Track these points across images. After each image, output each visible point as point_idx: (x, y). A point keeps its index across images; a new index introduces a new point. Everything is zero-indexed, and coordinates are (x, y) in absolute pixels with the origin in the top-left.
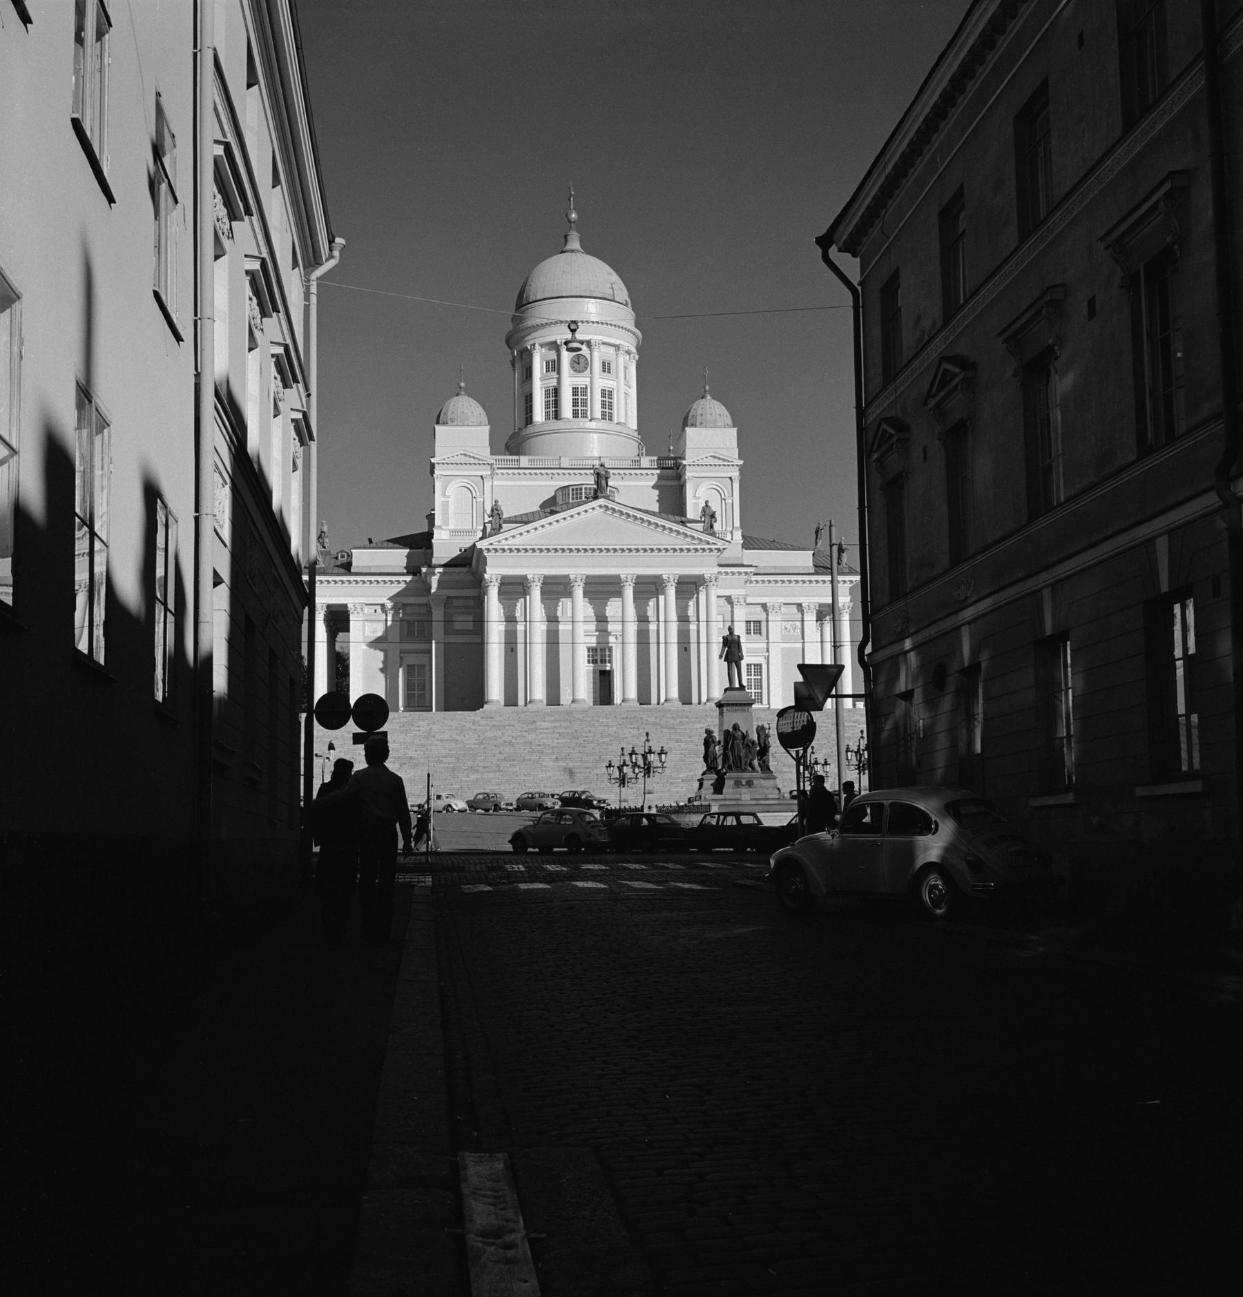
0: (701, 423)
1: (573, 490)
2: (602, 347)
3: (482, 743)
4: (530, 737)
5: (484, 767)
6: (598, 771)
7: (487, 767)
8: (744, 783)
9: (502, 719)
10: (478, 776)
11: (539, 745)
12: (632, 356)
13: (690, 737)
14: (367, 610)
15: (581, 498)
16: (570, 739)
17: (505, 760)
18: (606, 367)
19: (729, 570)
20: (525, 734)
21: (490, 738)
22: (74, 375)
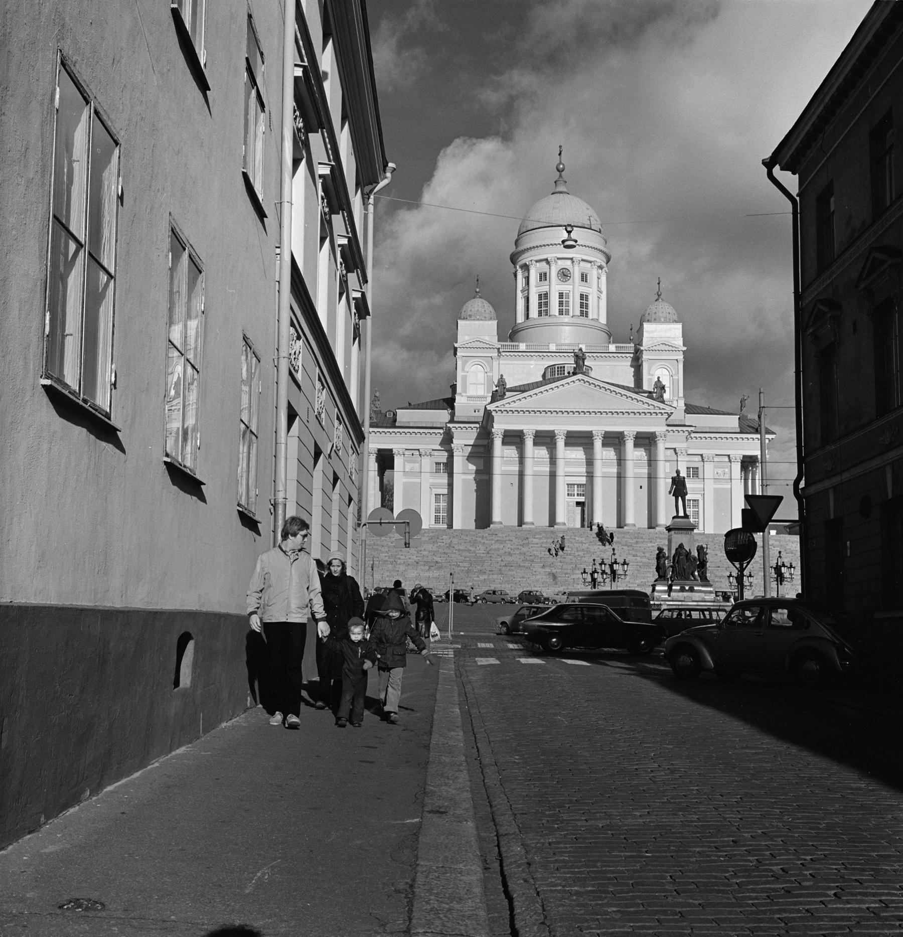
0: (655, 319)
1: (558, 368)
2: (582, 264)
3: (488, 553)
4: (524, 550)
5: (490, 571)
6: (574, 576)
7: (492, 571)
8: (687, 588)
12: (603, 270)
13: (644, 553)
15: (564, 374)
17: (505, 566)
18: (584, 278)
19: (675, 428)
20: (520, 547)
21: (495, 550)
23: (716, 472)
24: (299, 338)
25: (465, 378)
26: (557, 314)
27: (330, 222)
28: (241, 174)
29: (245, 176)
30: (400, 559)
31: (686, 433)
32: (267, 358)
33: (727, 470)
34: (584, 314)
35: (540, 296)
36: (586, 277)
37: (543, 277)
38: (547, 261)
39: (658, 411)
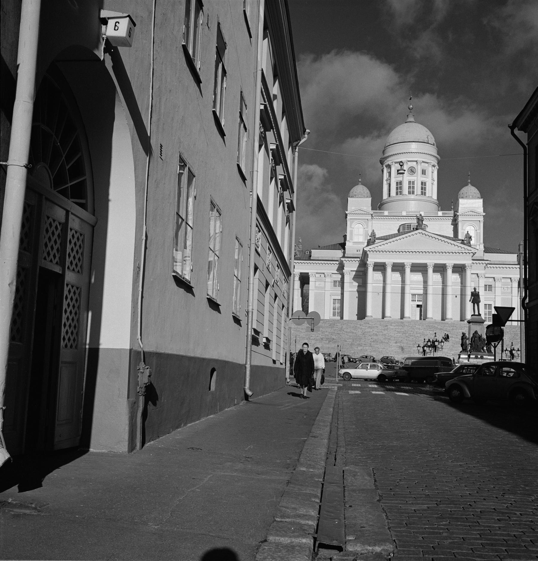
0: (466, 197)
1: (407, 225)
2: (423, 164)
3: (364, 334)
4: (385, 332)
5: (364, 344)
7: (365, 344)
8: (479, 357)
9: (373, 324)
10: (361, 348)
11: (389, 336)
12: (435, 167)
13: (457, 336)
14: (318, 275)
15: (411, 229)
16: (403, 334)
17: (374, 341)
18: (424, 172)
19: (477, 262)
20: (382, 331)
21: (368, 332)
22: (210, 199)
24: (259, 231)
25: (351, 232)
27: (275, 170)
29: (238, 165)
30: (312, 336)
31: (485, 265)
32: (245, 245)
34: (423, 193)
35: (397, 183)
36: (425, 172)
39: (467, 252)
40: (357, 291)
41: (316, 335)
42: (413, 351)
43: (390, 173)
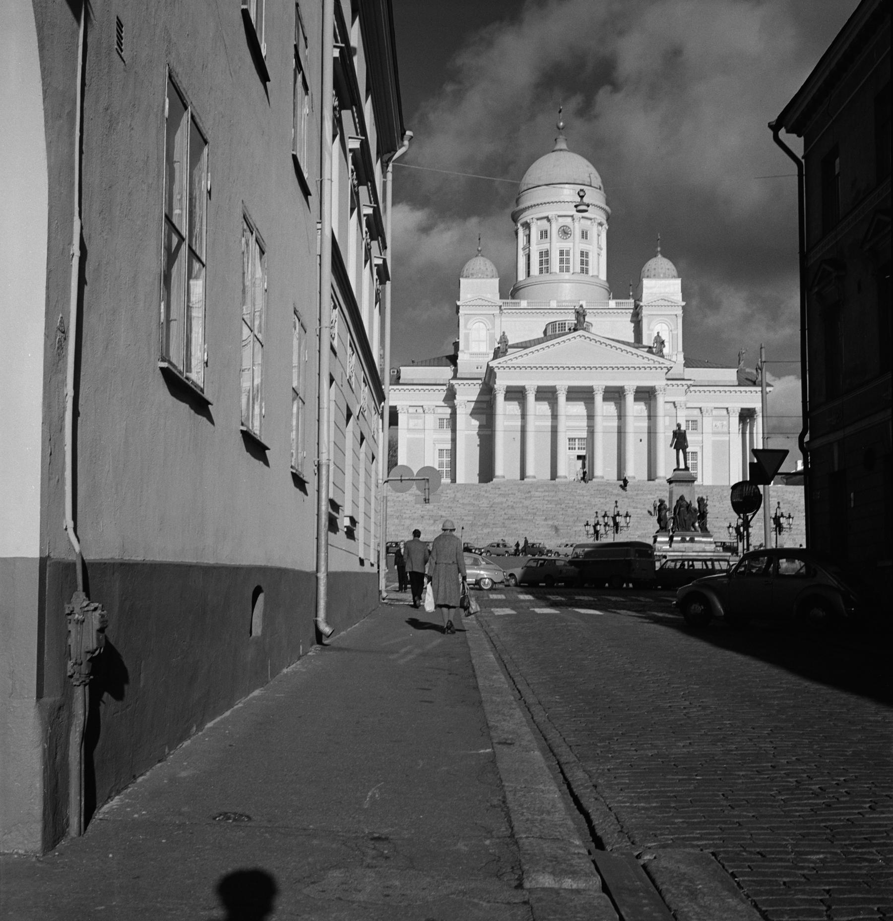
0: (654, 275)
1: (559, 324)
3: (491, 507)
4: (527, 503)
5: (493, 524)
8: (688, 539)
9: (507, 489)
11: (533, 509)
12: (603, 226)
14: (411, 410)
15: (565, 330)
16: (556, 505)
17: (508, 519)
18: (584, 235)
19: (674, 382)
20: (524, 501)
21: (498, 503)
22: (241, 210)
23: (714, 425)
24: (335, 307)
25: (467, 336)
26: (558, 271)
27: (357, 194)
28: (291, 157)
29: (295, 158)
30: (405, 513)
31: (686, 387)
32: (312, 327)
33: (725, 423)
34: (585, 271)
35: (541, 253)
36: (587, 234)
37: (544, 234)
38: (548, 219)
40: (478, 434)
41: (413, 511)
42: (574, 533)
43: (529, 236)
